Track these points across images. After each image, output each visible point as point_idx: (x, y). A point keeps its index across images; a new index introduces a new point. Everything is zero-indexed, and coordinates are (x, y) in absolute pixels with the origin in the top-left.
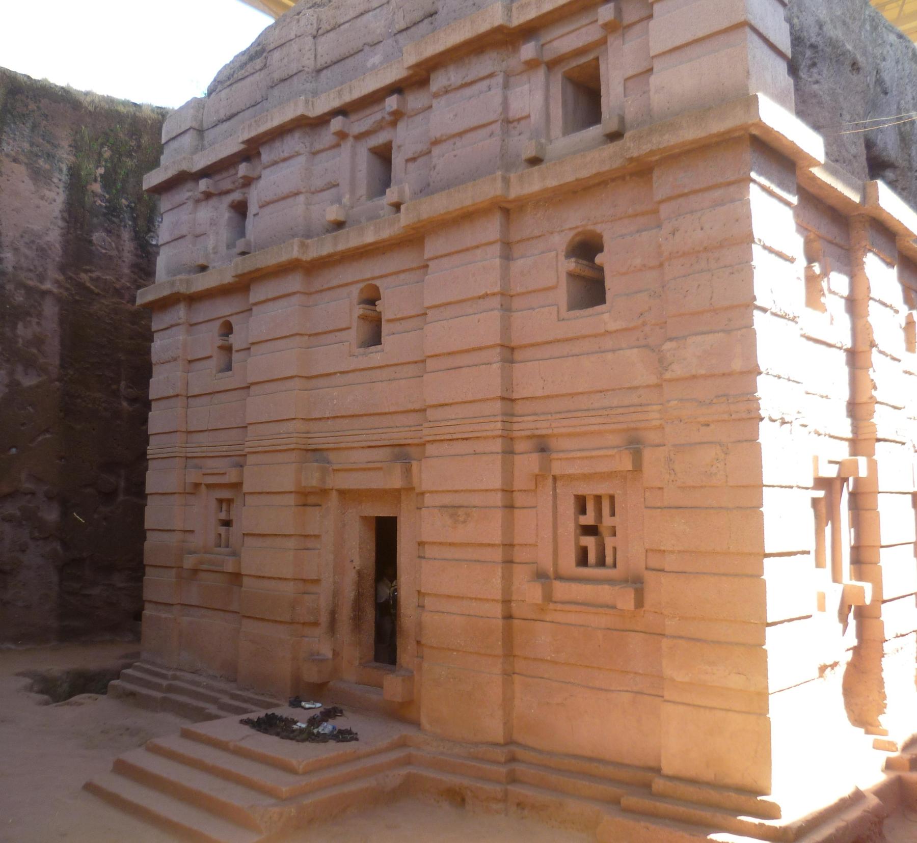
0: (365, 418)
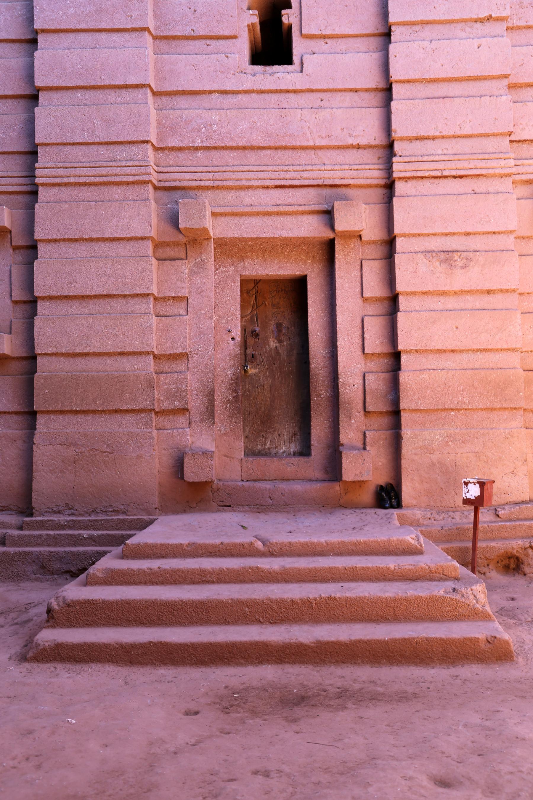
0: (268, 152)
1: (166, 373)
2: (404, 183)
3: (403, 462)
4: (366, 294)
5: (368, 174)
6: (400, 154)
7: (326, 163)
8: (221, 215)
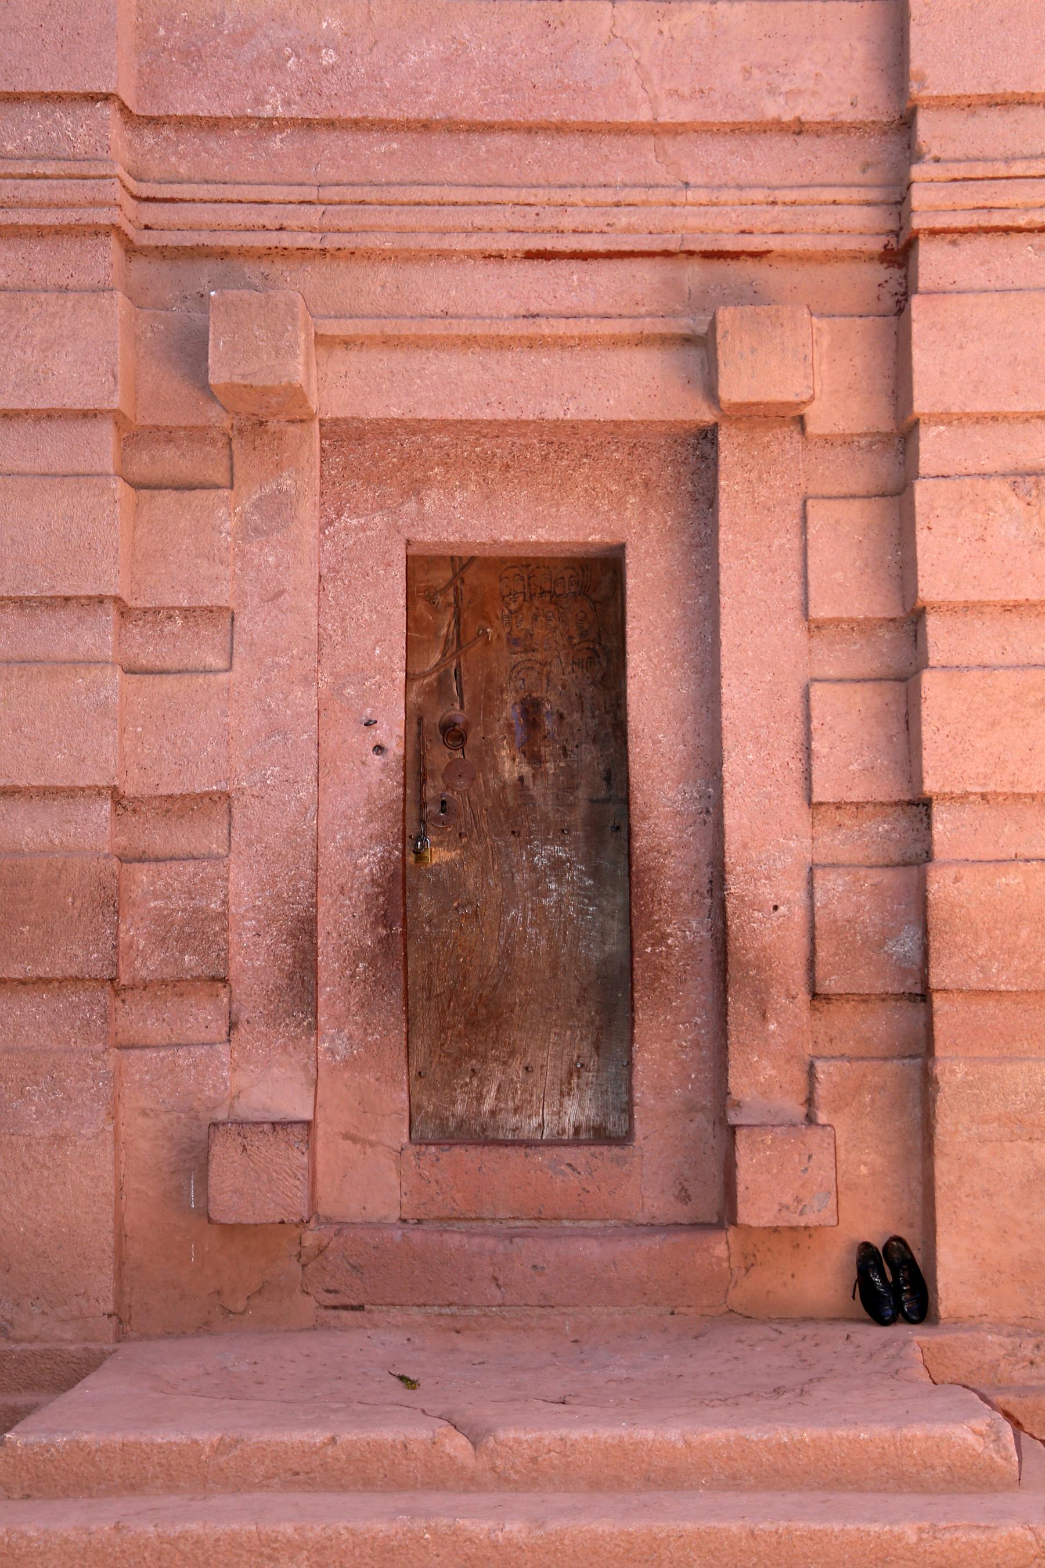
0: (503, 141)
1: (157, 860)
2: (948, 248)
3: (941, 1165)
4: (820, 611)
5: (827, 218)
6: (935, 152)
7: (692, 180)
8: (347, 343)
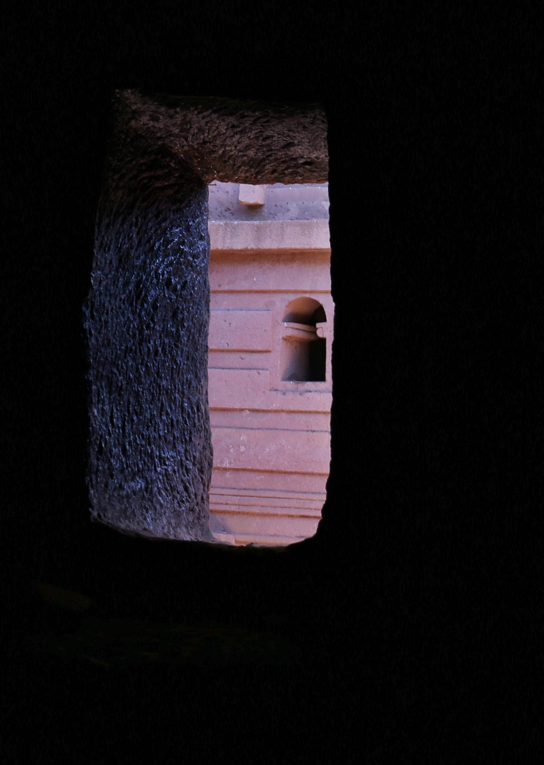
0: (295, 477)
